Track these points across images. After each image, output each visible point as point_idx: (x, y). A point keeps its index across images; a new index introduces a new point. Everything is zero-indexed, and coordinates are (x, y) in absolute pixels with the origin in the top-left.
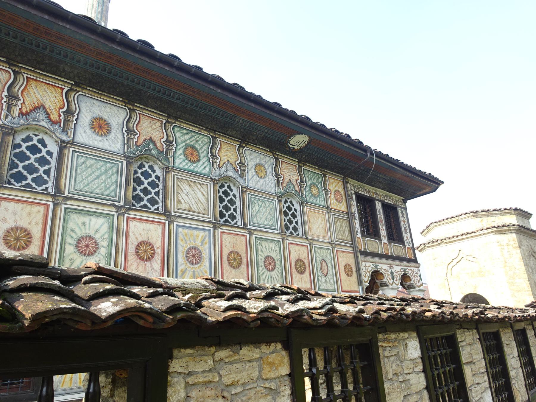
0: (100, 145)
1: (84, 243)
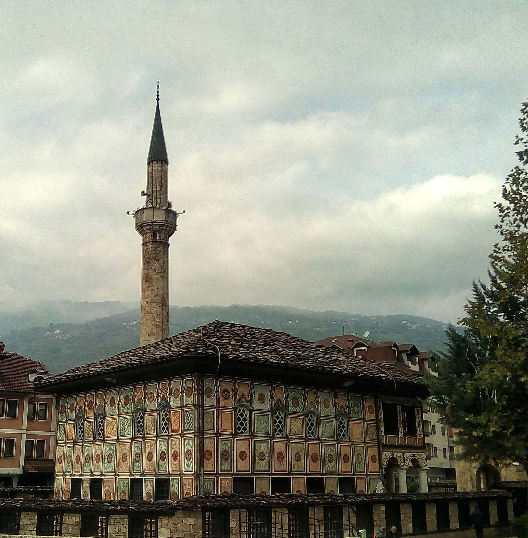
0: (262, 408)
1: (261, 455)
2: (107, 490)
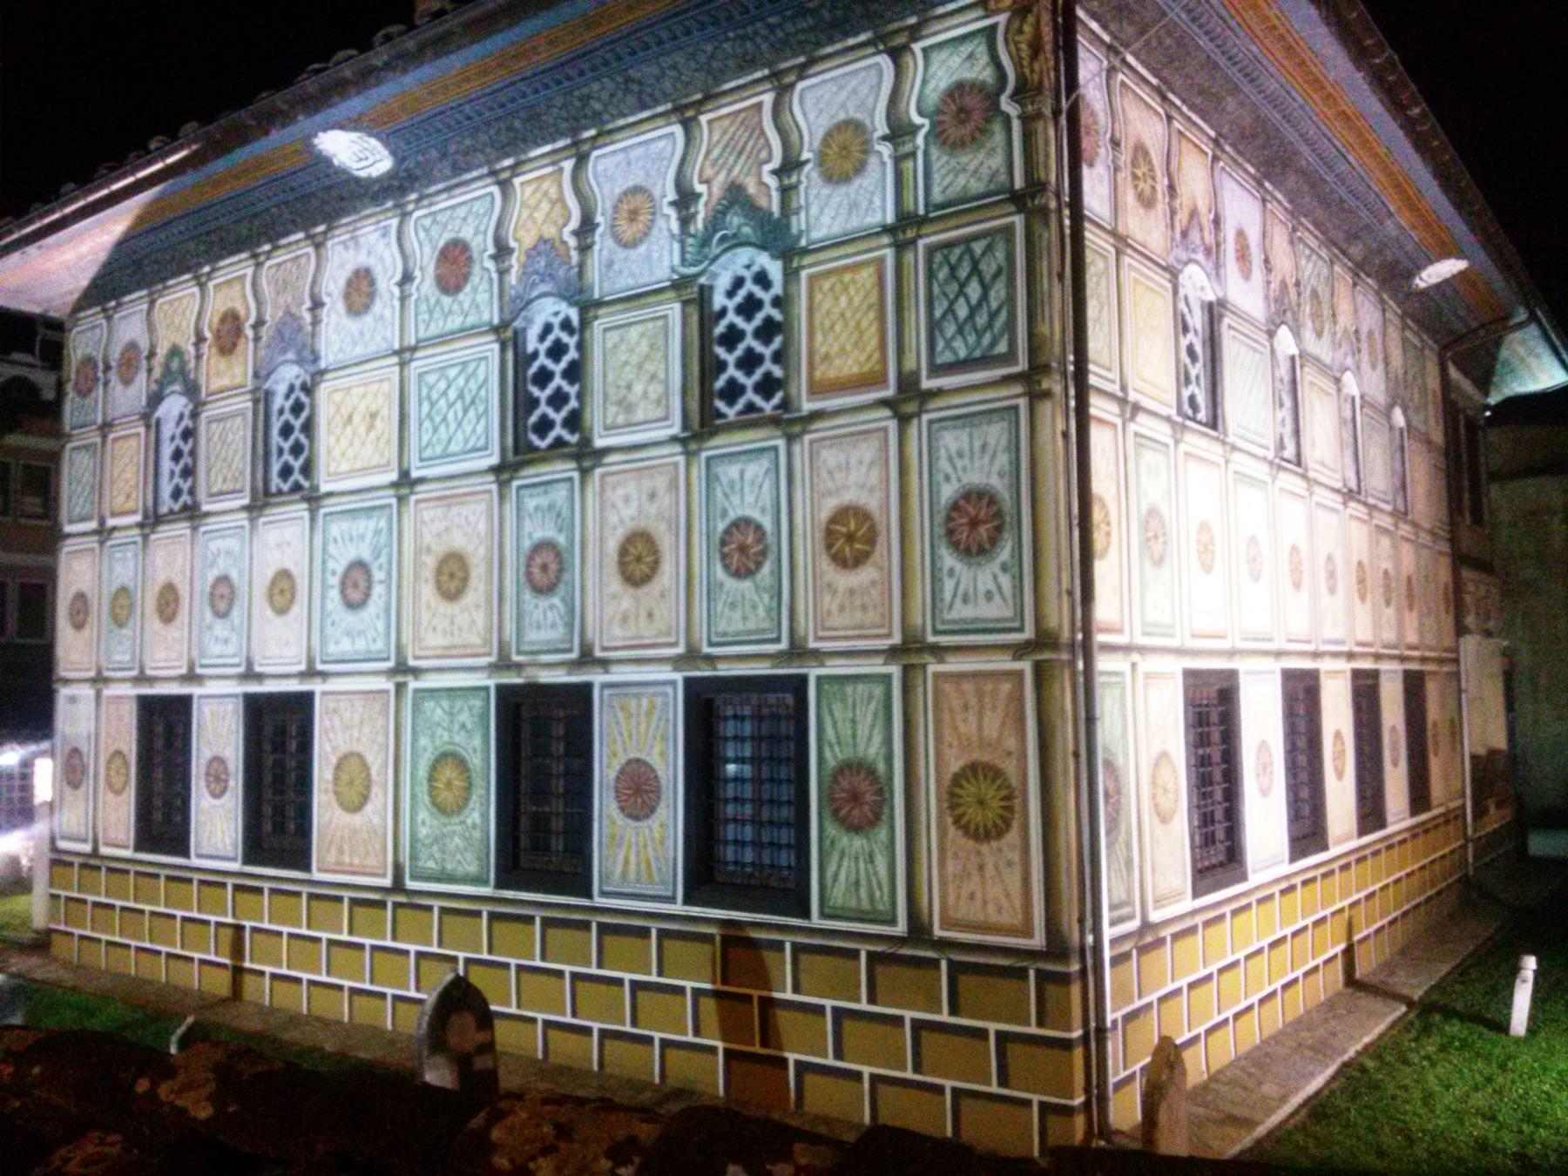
2: (344, 748)
